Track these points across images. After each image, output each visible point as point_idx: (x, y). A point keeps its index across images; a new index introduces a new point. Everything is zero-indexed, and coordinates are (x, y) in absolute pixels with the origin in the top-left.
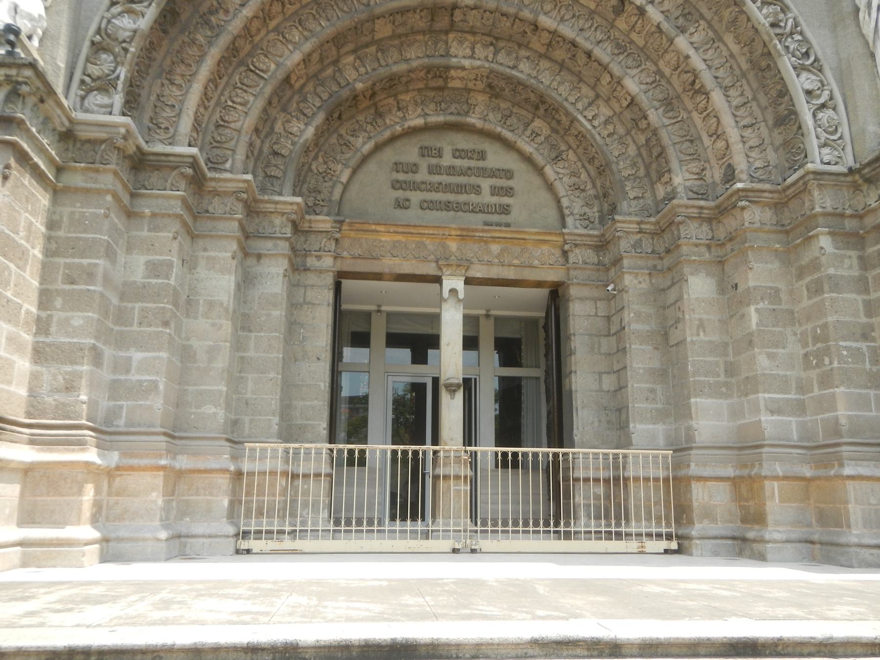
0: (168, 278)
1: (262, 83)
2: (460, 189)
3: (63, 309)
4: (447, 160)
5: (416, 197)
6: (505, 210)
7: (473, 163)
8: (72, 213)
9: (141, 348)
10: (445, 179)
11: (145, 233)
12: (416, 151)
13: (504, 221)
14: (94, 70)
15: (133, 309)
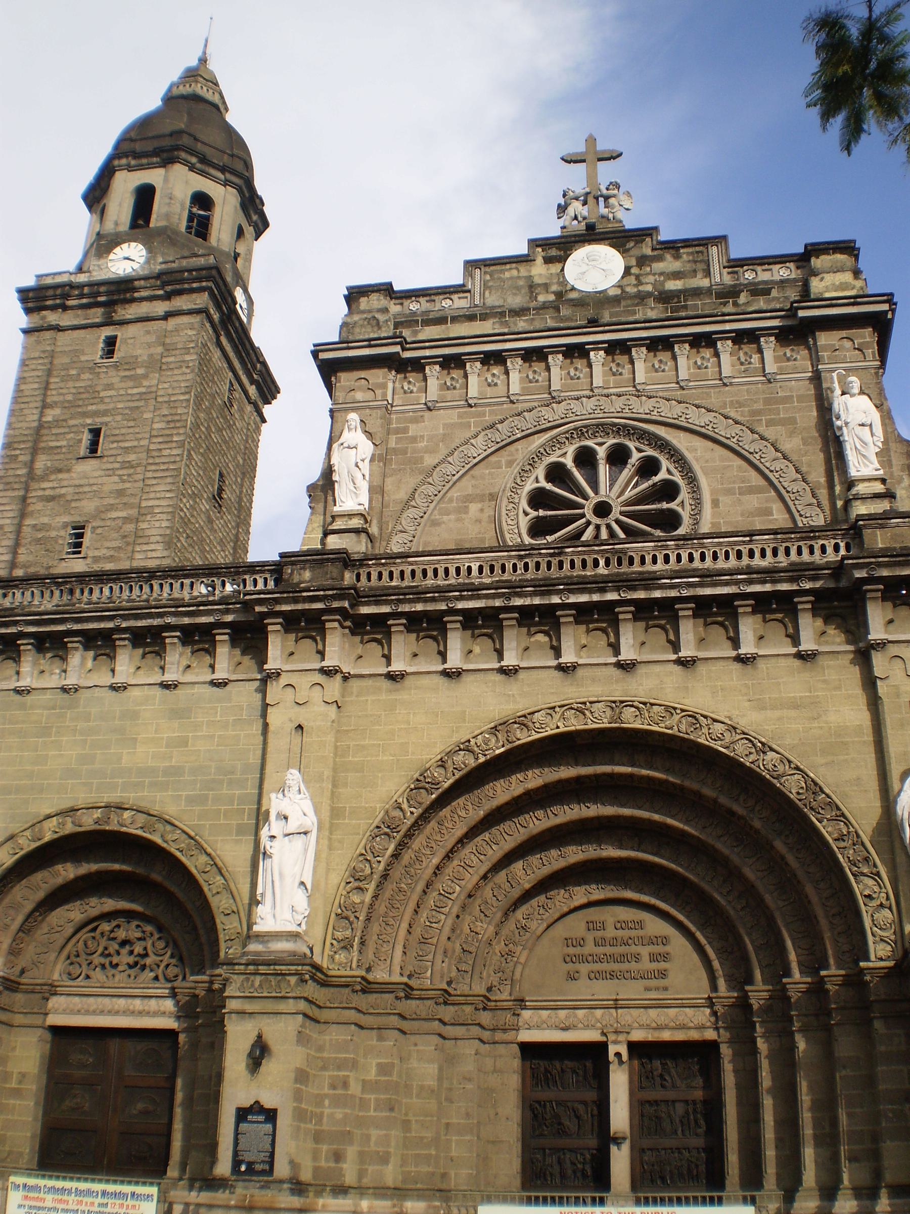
0: (391, 1075)
1: (450, 902)
2: (623, 958)
3: (329, 1106)
4: (610, 932)
5: (584, 968)
6: (663, 974)
7: (633, 933)
8: (331, 1040)
9: (377, 1127)
10: (608, 950)
11: (375, 1042)
12: (583, 925)
13: (662, 985)
14: (339, 935)
15: (370, 1099)
